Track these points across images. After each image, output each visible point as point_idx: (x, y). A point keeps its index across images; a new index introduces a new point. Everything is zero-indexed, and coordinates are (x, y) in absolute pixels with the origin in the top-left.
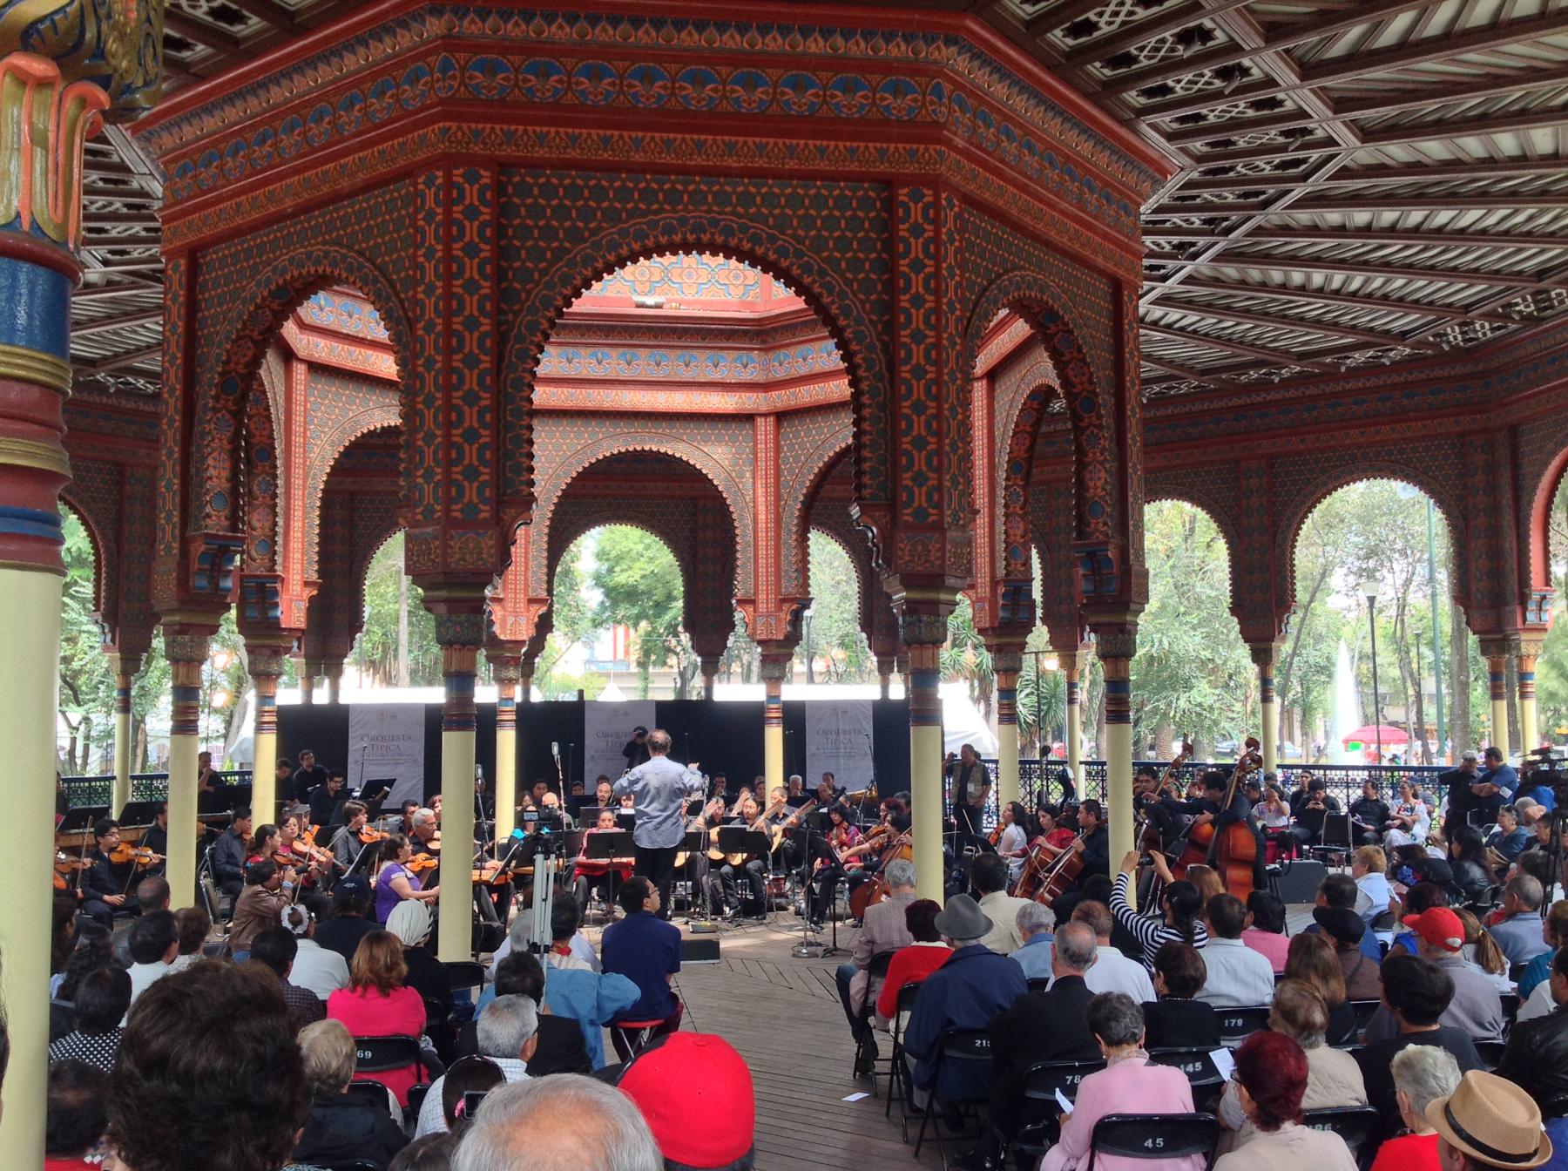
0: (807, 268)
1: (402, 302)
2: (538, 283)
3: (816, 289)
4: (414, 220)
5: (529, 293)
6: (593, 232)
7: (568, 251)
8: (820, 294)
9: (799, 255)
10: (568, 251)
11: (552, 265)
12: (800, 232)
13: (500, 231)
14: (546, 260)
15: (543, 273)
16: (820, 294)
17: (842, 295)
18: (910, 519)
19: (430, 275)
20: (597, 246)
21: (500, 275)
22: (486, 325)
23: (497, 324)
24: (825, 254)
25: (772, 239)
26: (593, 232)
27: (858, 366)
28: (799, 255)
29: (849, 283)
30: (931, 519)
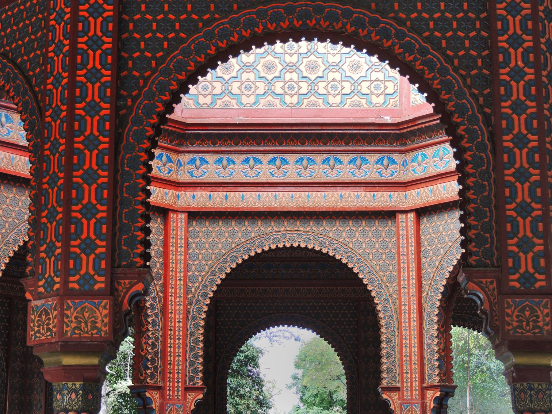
0: (408, 48)
1: (35, 94)
2: (154, 71)
3: (418, 66)
4: (47, 20)
5: (146, 79)
6: (207, 23)
7: (182, 41)
8: (423, 71)
9: (400, 35)
10: (182, 41)
11: (168, 54)
12: (402, 15)
13: (121, 26)
14: (163, 50)
15: (160, 61)
16: (423, 71)
17: (443, 71)
18: (517, 285)
19: (58, 68)
20: (209, 36)
21: (119, 65)
22: (106, 110)
23: (116, 109)
24: (427, 34)
25: (375, 22)
26: (207, 23)
27: (462, 137)
28: (400, 35)
29: (450, 60)
30: (538, 285)
